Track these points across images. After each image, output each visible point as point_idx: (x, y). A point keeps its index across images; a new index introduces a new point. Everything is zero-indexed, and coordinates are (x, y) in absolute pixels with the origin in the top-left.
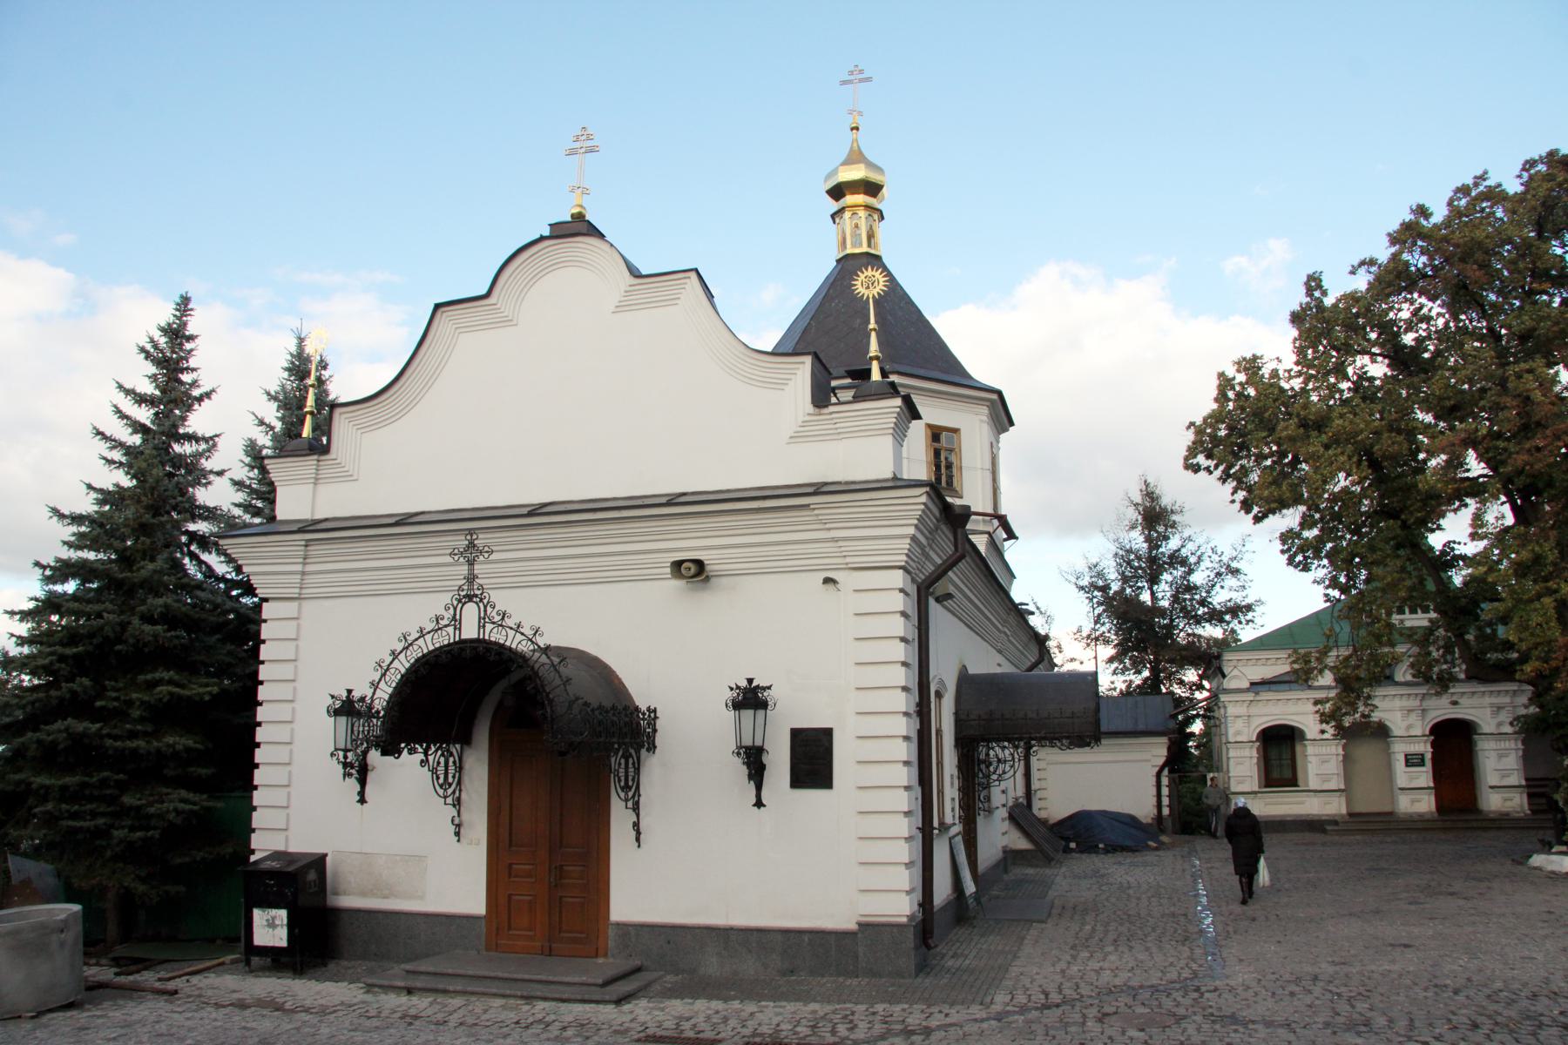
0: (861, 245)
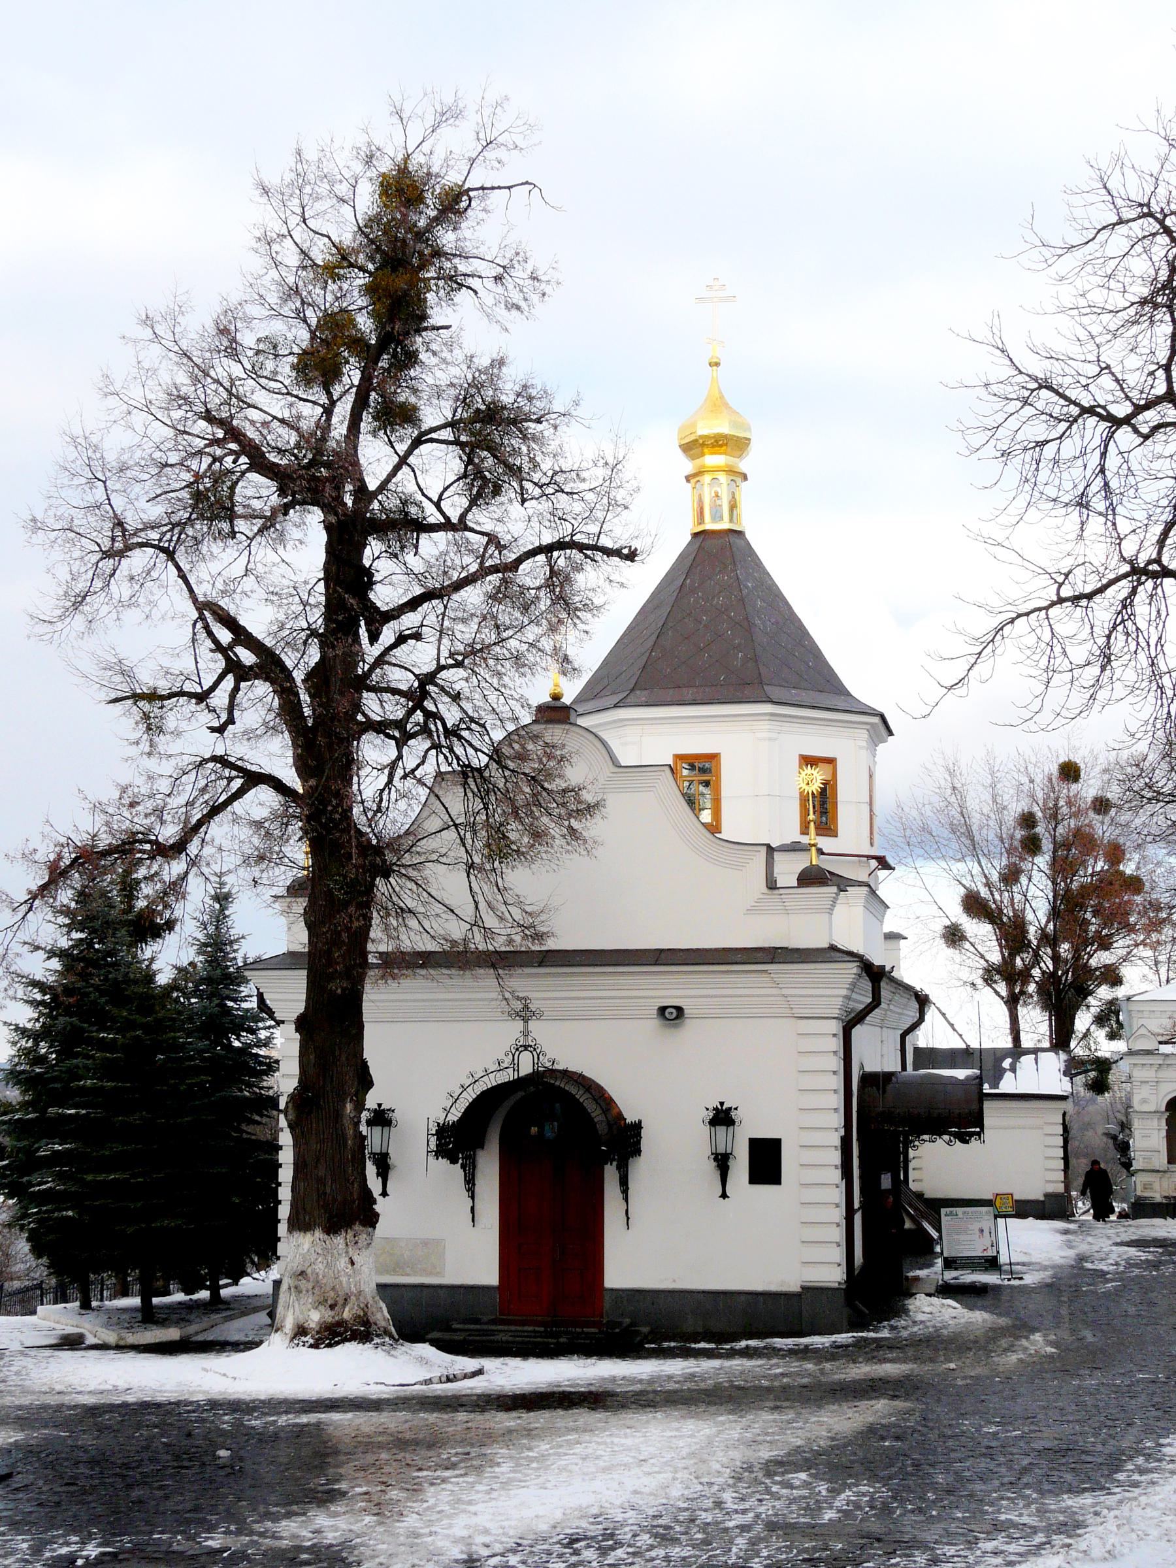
0: (721, 518)
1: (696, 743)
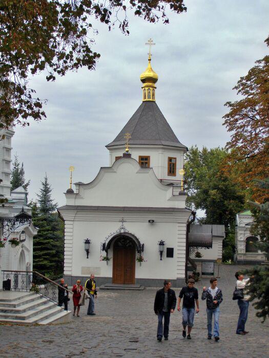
1: (144, 153)
